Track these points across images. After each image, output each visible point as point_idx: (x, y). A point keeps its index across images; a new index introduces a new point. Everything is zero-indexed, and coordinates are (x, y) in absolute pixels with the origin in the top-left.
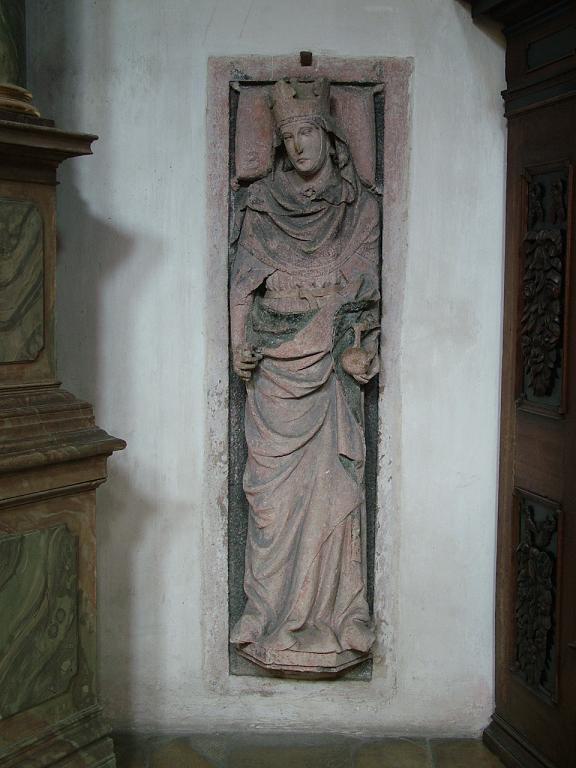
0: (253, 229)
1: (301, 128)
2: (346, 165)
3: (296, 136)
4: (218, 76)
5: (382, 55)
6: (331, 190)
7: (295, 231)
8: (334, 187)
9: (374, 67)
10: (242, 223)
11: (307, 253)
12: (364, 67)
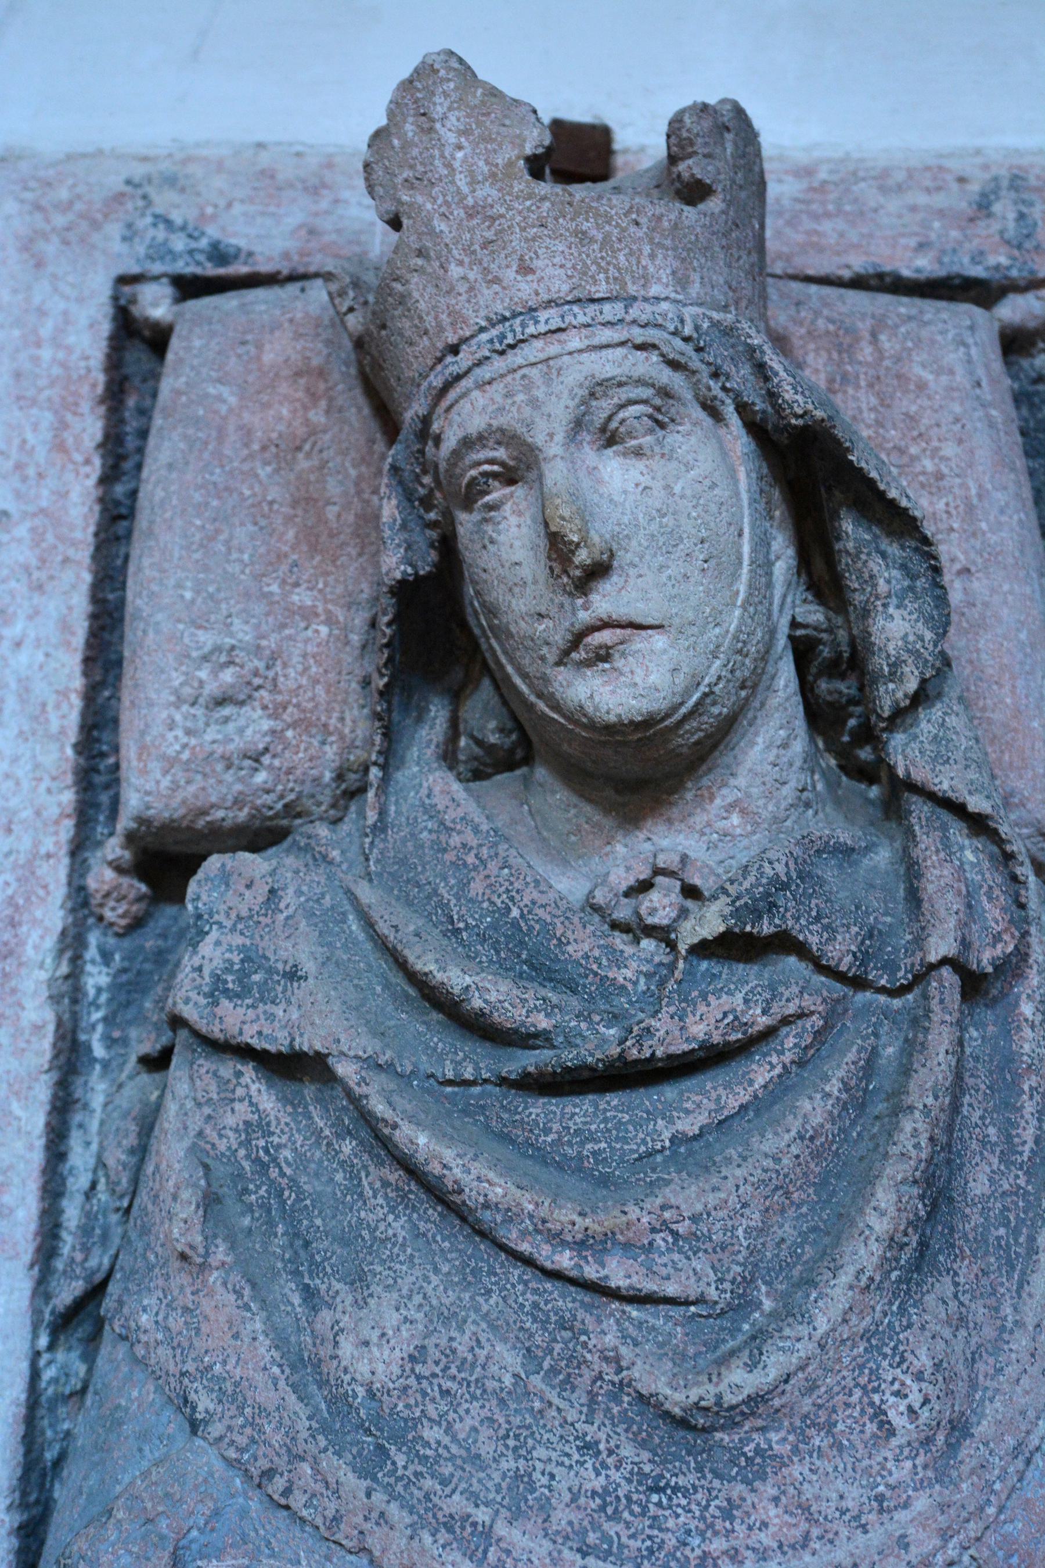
0: (210, 1201)
1: (598, 388)
2: (920, 698)
3: (554, 449)
4: (50, 248)
5: (1012, 140)
6: (829, 872)
7: (565, 1215)
8: (846, 853)
9: (984, 206)
10: (141, 1151)
11: (683, 1423)
12: (922, 199)
